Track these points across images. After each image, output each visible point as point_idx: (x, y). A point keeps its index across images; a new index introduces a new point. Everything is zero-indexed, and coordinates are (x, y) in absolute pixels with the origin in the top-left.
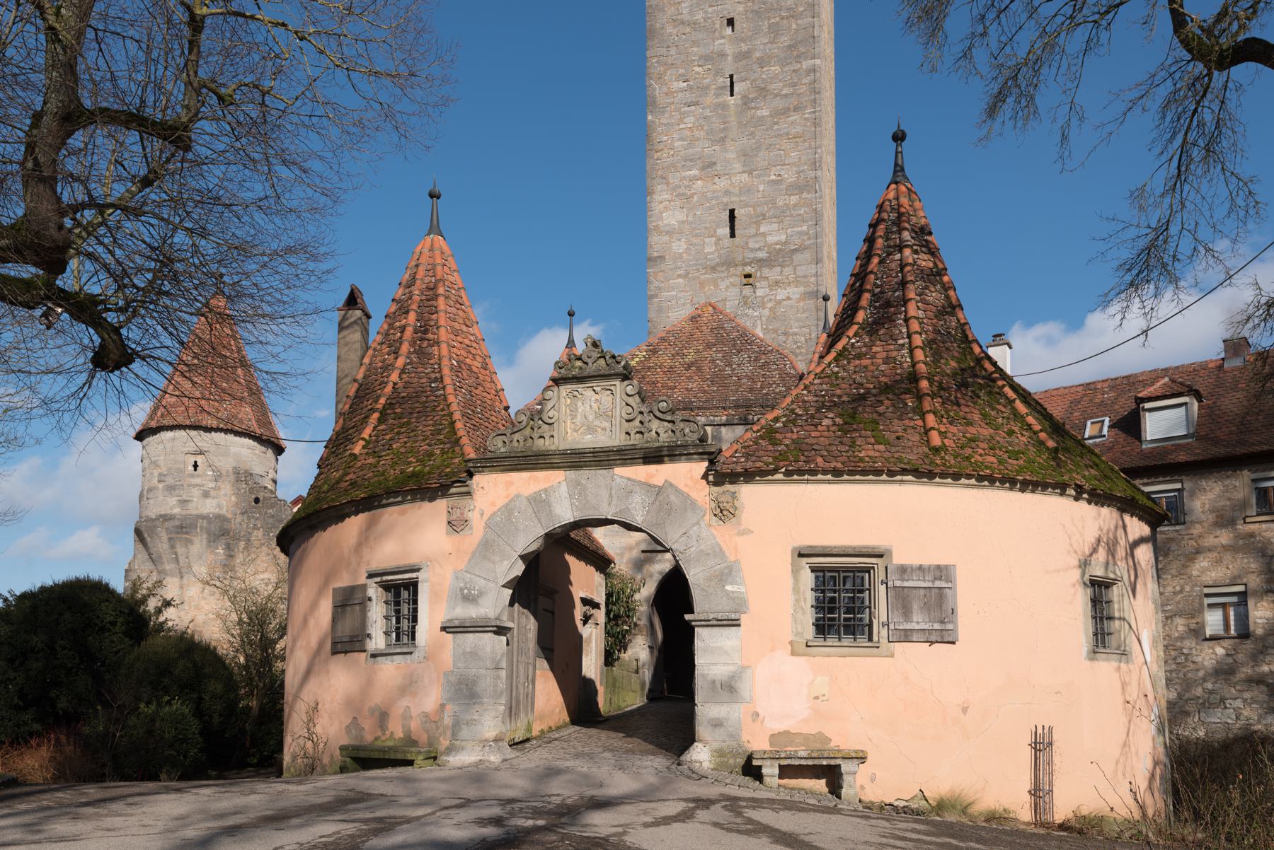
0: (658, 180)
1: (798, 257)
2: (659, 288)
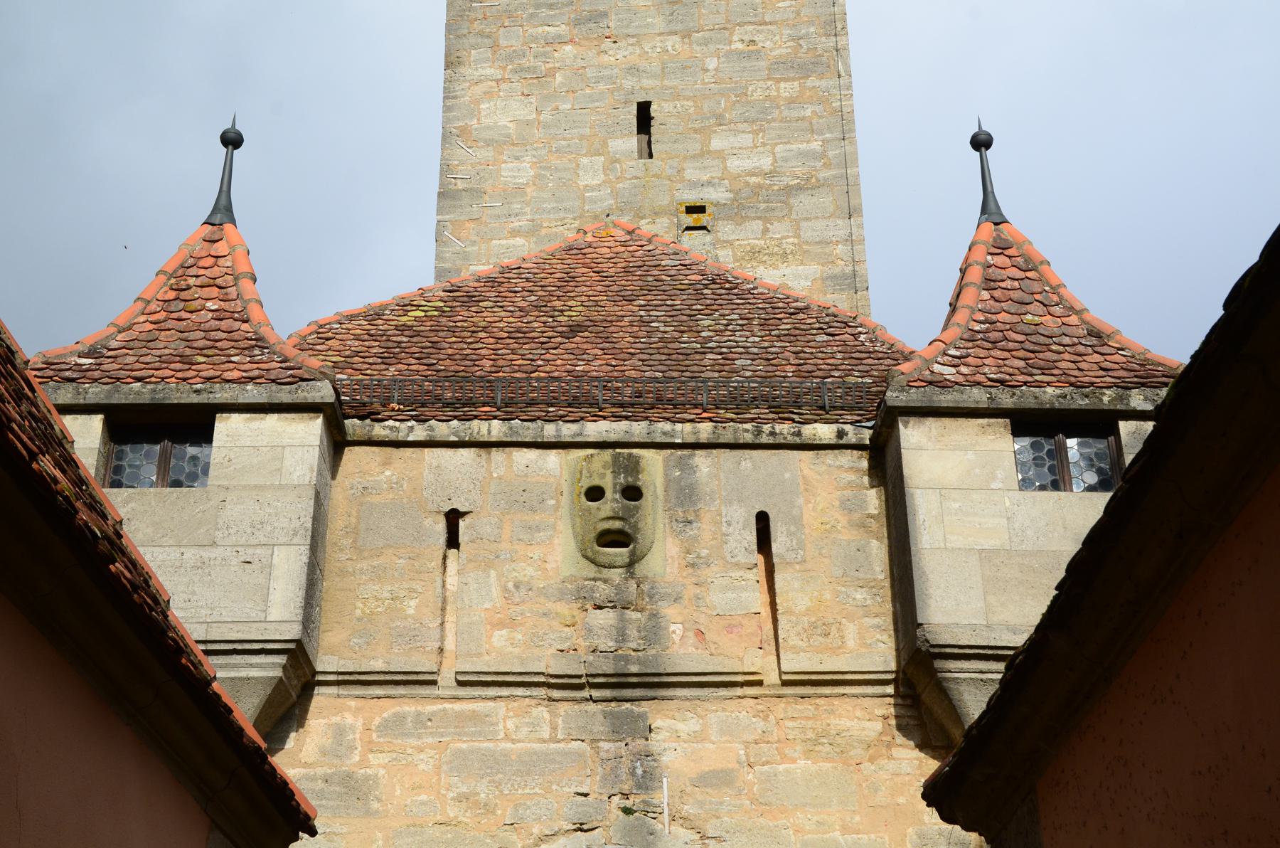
0: (472, 40)
1: (803, 203)
2: (466, 257)
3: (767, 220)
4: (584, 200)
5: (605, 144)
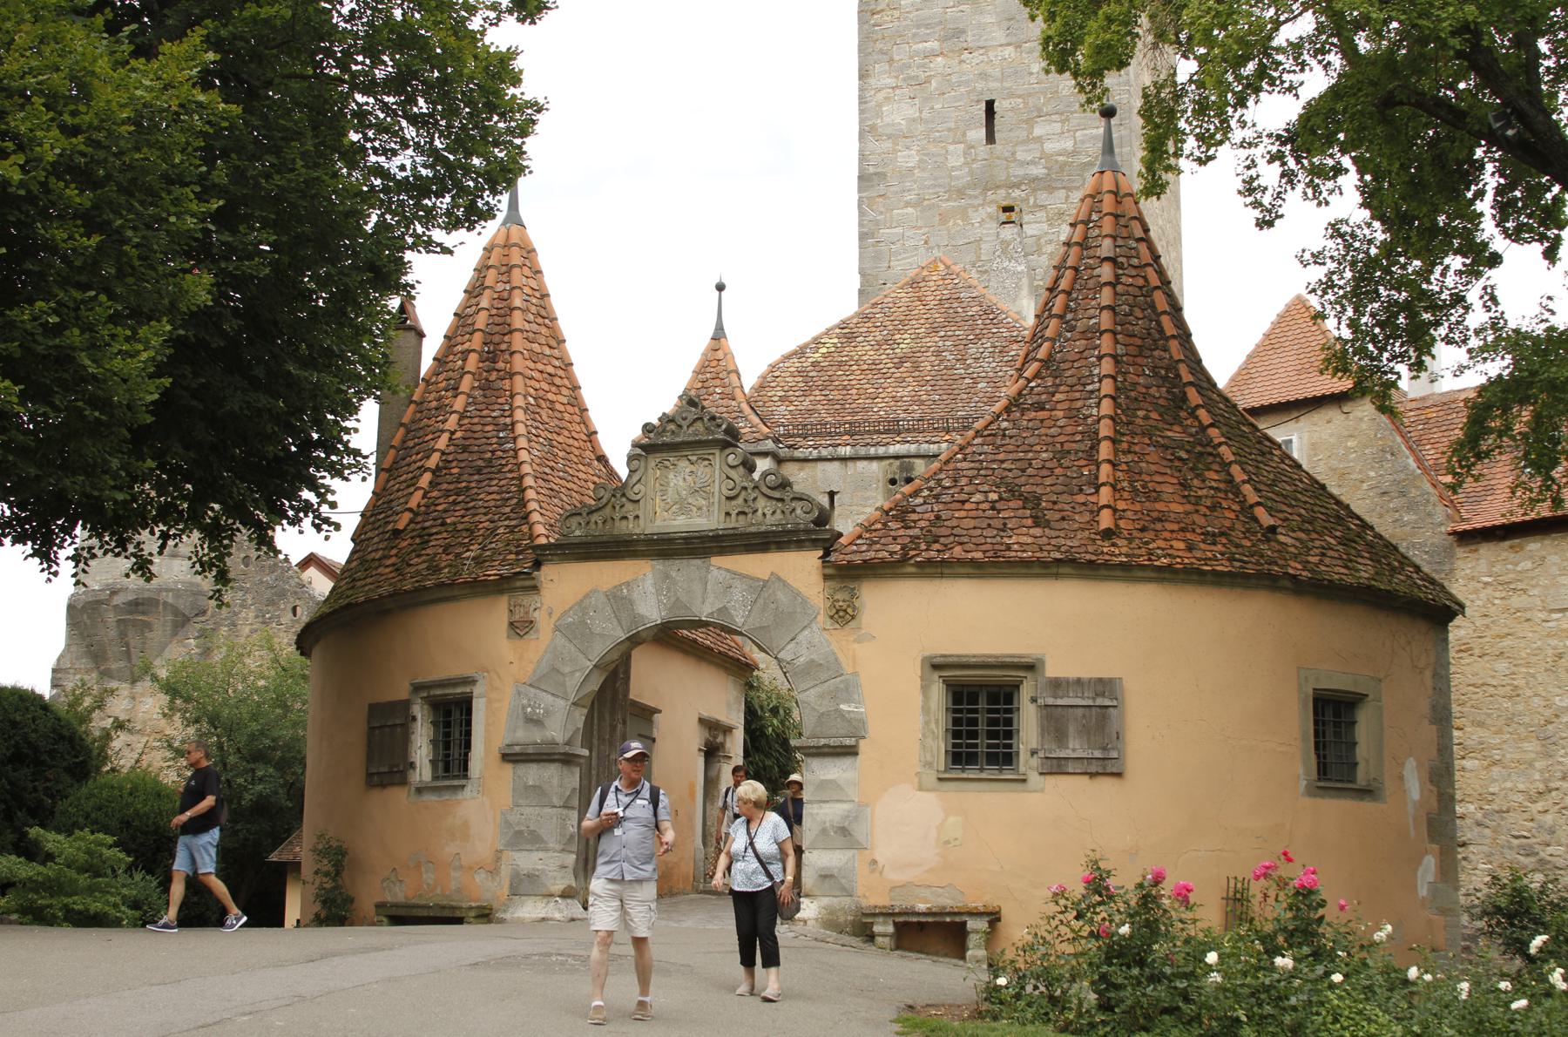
2: (877, 222)
3: (1069, 189)
4: (950, 176)
5: (964, 134)
